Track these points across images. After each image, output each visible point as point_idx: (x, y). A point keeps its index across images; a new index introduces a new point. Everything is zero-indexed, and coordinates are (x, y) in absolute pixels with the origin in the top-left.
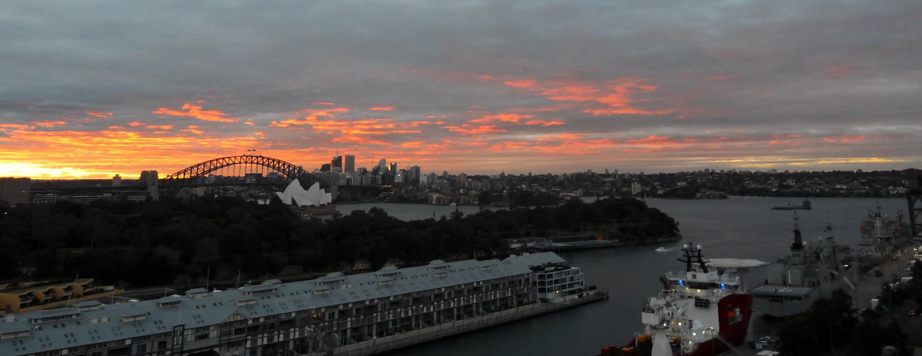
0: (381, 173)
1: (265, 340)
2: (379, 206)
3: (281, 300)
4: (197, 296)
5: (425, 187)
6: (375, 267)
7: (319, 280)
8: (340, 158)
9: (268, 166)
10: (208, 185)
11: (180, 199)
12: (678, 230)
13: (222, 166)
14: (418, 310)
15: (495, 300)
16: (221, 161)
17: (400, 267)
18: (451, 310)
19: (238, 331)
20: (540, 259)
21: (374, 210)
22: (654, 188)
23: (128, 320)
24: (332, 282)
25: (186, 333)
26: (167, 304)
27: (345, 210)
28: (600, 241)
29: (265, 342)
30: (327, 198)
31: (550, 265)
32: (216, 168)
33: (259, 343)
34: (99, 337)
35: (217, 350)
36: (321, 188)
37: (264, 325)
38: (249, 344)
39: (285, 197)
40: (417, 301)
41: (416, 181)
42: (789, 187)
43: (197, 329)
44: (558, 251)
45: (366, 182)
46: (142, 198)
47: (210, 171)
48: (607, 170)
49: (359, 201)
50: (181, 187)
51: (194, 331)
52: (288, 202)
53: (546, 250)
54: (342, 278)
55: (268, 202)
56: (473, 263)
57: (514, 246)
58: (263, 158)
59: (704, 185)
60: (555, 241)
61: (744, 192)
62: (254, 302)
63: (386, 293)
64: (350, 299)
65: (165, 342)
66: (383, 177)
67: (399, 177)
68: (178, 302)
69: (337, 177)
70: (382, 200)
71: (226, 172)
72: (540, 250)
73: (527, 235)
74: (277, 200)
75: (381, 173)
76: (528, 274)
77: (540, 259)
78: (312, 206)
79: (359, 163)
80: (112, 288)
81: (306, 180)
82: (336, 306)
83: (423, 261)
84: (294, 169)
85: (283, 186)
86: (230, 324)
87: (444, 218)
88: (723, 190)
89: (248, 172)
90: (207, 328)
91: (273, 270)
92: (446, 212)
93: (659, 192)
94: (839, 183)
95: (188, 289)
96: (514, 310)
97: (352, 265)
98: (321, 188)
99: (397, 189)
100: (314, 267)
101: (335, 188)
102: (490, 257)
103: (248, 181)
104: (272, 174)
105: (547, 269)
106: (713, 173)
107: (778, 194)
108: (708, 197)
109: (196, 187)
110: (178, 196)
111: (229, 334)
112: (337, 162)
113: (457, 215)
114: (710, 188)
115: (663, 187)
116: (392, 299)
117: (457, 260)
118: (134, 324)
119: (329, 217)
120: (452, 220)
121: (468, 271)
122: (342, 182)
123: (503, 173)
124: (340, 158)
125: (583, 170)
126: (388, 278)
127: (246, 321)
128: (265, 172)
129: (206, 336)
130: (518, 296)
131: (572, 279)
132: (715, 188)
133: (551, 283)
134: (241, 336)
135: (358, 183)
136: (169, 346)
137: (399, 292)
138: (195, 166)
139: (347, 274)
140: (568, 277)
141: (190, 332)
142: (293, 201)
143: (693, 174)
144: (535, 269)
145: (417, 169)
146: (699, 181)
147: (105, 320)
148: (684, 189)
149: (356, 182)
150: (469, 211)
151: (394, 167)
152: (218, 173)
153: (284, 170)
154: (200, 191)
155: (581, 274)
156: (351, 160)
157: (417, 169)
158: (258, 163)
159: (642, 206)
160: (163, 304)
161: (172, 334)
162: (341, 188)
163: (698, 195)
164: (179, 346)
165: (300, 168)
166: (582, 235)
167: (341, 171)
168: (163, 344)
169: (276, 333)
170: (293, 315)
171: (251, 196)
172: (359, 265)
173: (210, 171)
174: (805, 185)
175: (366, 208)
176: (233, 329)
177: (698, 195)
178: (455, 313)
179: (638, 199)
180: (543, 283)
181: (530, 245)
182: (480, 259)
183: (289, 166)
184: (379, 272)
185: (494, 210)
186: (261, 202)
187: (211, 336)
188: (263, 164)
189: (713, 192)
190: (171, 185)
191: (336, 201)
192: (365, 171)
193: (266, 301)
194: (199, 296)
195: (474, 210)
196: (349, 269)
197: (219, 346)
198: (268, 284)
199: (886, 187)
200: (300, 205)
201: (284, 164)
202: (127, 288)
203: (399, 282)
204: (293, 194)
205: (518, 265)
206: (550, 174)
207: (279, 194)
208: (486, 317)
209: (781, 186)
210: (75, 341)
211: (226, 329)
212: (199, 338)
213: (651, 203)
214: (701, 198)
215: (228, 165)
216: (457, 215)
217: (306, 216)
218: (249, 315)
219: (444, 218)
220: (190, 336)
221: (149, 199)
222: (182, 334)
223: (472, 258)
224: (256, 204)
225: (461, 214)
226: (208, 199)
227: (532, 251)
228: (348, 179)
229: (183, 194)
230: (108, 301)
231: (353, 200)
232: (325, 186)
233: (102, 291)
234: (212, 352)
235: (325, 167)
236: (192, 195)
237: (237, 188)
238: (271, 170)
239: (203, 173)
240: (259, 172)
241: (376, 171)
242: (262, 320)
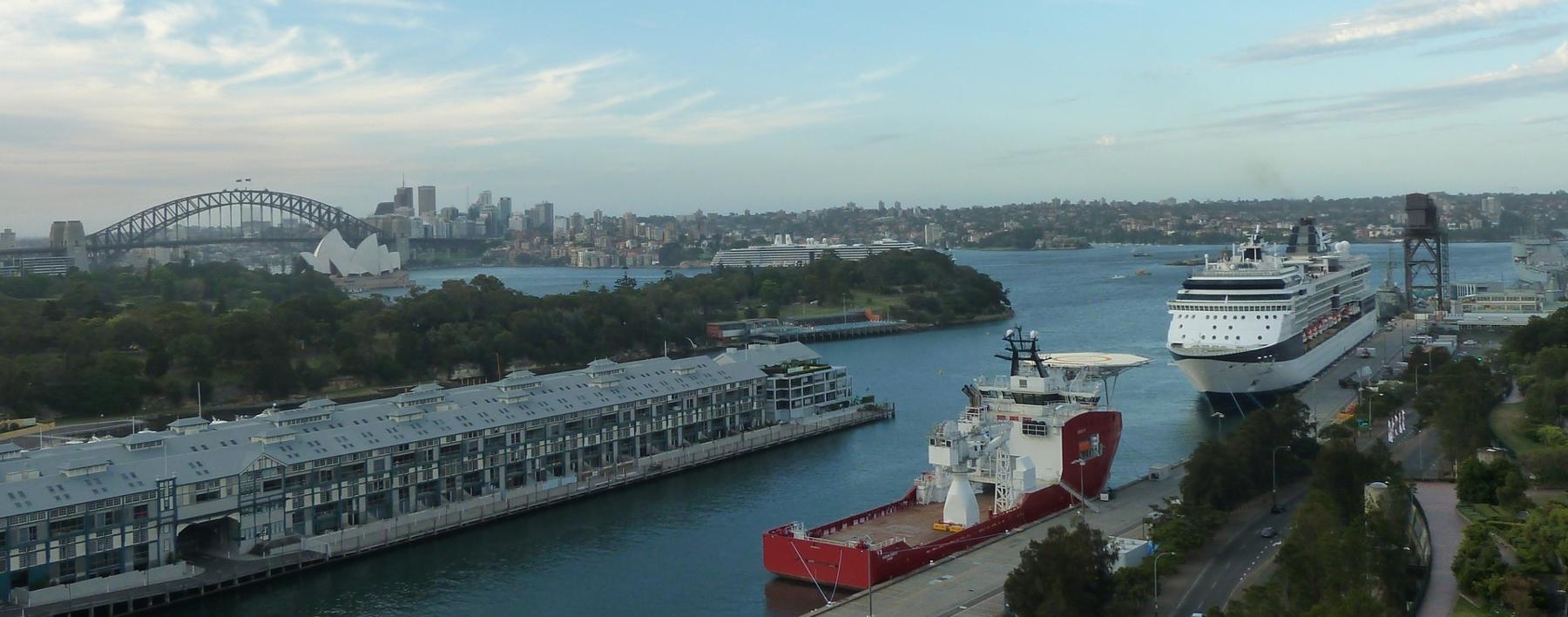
0: (483, 215)
1: (318, 498)
2: (488, 272)
3: (338, 432)
4: (186, 431)
5: (564, 240)
6: (491, 374)
7: (400, 398)
8: (410, 190)
9: (282, 207)
10: (175, 245)
11: (130, 269)
12: (1008, 303)
13: (198, 210)
14: (575, 442)
15: (703, 425)
16: (195, 201)
17: (538, 373)
18: (629, 441)
19: (269, 485)
20: (775, 354)
21: (480, 279)
22: (963, 232)
23: (75, 474)
24: (423, 401)
25: (178, 491)
26: (140, 445)
27: (432, 280)
28: (876, 322)
29: (318, 502)
30: (393, 260)
31: (795, 363)
32: (188, 214)
33: (308, 503)
34: (28, 503)
35: (235, 516)
36: (381, 242)
37: (314, 474)
38: (289, 506)
39: (318, 259)
40: (572, 427)
41: (546, 229)
42: (1196, 227)
43: (198, 485)
44: (807, 339)
45: (459, 230)
46: (61, 269)
47: (176, 218)
48: (881, 204)
49: (449, 265)
50: (129, 246)
51: (193, 489)
52: (323, 268)
53: (783, 340)
54: (440, 393)
55: (288, 270)
56: (664, 362)
57: (727, 333)
58: (271, 194)
59: (1050, 228)
60: (799, 323)
61: (1120, 236)
62: (292, 438)
63: (521, 417)
64: (458, 429)
65: (145, 507)
66: (488, 222)
67: (516, 224)
68: (159, 442)
69: (405, 224)
70: (487, 261)
71: (202, 221)
72: (772, 339)
73: (752, 314)
74: (301, 264)
75: (483, 215)
76: (759, 380)
77: (775, 354)
78: (367, 274)
79: (441, 204)
80: (32, 421)
81: (353, 232)
82: (523, 424)
83: (575, 359)
84: (328, 212)
85: (312, 243)
86: (257, 474)
87: (603, 289)
88: (1083, 234)
89: (247, 219)
90: (217, 481)
91: (315, 385)
92: (609, 279)
93: (972, 239)
94: (1283, 220)
95: (172, 419)
96: (738, 438)
97: (451, 372)
98: (381, 242)
99: (516, 244)
100: (386, 376)
101: (404, 242)
102: (687, 353)
103: (247, 235)
104: (292, 221)
105: (790, 371)
106: (1066, 205)
107: (1177, 239)
108: (1056, 246)
109: (153, 245)
110: (124, 264)
111: (255, 490)
112: (404, 196)
113: (628, 284)
114: (1060, 232)
115: (977, 229)
116: (488, 433)
117: (631, 360)
118: (87, 480)
119: (404, 293)
120: (618, 292)
121: (657, 377)
122: (416, 233)
123: (700, 212)
124: (410, 190)
125: (840, 202)
126: (519, 392)
127: (280, 469)
128: (275, 218)
129: (214, 496)
130: (742, 415)
131: (833, 385)
132: (1071, 232)
133: (798, 392)
134: (275, 494)
135: (444, 235)
136: (152, 513)
137: (541, 413)
138: (148, 211)
139: (446, 387)
140: (826, 383)
141: (186, 490)
142: (334, 269)
143: (1030, 207)
144: (770, 371)
145: (548, 207)
146: (1041, 219)
147: (33, 474)
148: (1017, 232)
149: (439, 233)
150: (648, 275)
151: (506, 203)
152: (193, 221)
153: (311, 214)
154: (162, 256)
155: (848, 377)
156: (428, 194)
157: (548, 207)
158: (262, 204)
159: (946, 262)
160: (133, 446)
161: (159, 492)
162: (413, 242)
163: (1039, 243)
164: (170, 513)
165: (339, 212)
166: (844, 313)
167: (412, 213)
168: (141, 511)
169: (335, 486)
170: (459, 438)
171: (255, 260)
172: (462, 373)
173: (176, 218)
174: (1225, 223)
175: (467, 275)
176: (260, 483)
177: (1039, 243)
178: (638, 447)
179: (941, 251)
180: (785, 394)
181: (754, 331)
182: (672, 356)
183: (319, 208)
184: (502, 383)
185: (690, 275)
186: (276, 270)
187: (223, 494)
188: (272, 205)
189: (1065, 238)
190: (110, 244)
191: (410, 265)
192: (453, 214)
193: (312, 436)
194: (196, 430)
195: (657, 276)
196: (444, 378)
197: (239, 510)
198: (310, 406)
199: (1363, 225)
200: (345, 274)
201: (319, 208)
202: (58, 421)
203: (540, 397)
204: (329, 254)
205: (734, 365)
206: (782, 212)
207: (303, 254)
208: (690, 450)
209: (1182, 226)
210: (67, 497)
211: (247, 482)
212: (201, 498)
213: (959, 256)
214: (1044, 248)
215: (209, 207)
216: (628, 284)
217: (357, 294)
218: (284, 459)
219: (603, 289)
220: (185, 495)
221: (73, 269)
222: (173, 493)
223: (656, 354)
224: (265, 274)
225: (633, 282)
226: (181, 269)
227: (761, 339)
228: (426, 228)
229: (134, 259)
230: (32, 443)
231: (438, 264)
232: (387, 240)
233: (15, 427)
234: (227, 519)
235: (383, 208)
236: (150, 261)
237: (227, 247)
238: (287, 215)
239: (165, 223)
240: (266, 218)
241: (474, 213)
242: (308, 467)
